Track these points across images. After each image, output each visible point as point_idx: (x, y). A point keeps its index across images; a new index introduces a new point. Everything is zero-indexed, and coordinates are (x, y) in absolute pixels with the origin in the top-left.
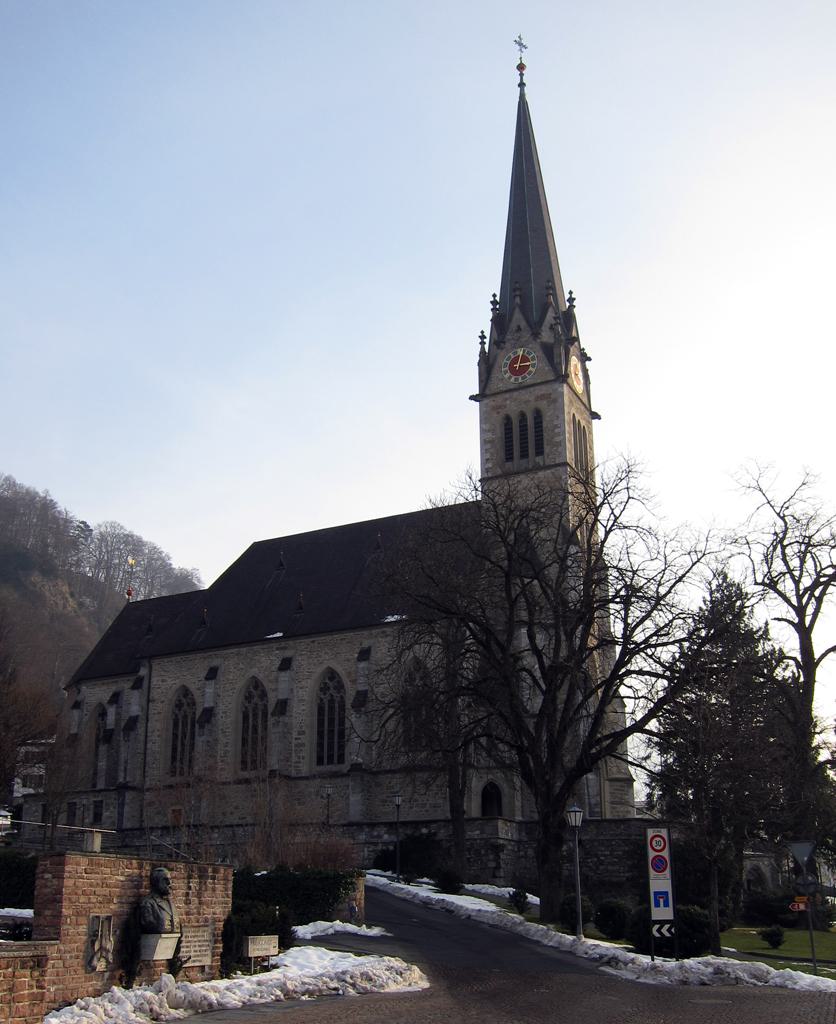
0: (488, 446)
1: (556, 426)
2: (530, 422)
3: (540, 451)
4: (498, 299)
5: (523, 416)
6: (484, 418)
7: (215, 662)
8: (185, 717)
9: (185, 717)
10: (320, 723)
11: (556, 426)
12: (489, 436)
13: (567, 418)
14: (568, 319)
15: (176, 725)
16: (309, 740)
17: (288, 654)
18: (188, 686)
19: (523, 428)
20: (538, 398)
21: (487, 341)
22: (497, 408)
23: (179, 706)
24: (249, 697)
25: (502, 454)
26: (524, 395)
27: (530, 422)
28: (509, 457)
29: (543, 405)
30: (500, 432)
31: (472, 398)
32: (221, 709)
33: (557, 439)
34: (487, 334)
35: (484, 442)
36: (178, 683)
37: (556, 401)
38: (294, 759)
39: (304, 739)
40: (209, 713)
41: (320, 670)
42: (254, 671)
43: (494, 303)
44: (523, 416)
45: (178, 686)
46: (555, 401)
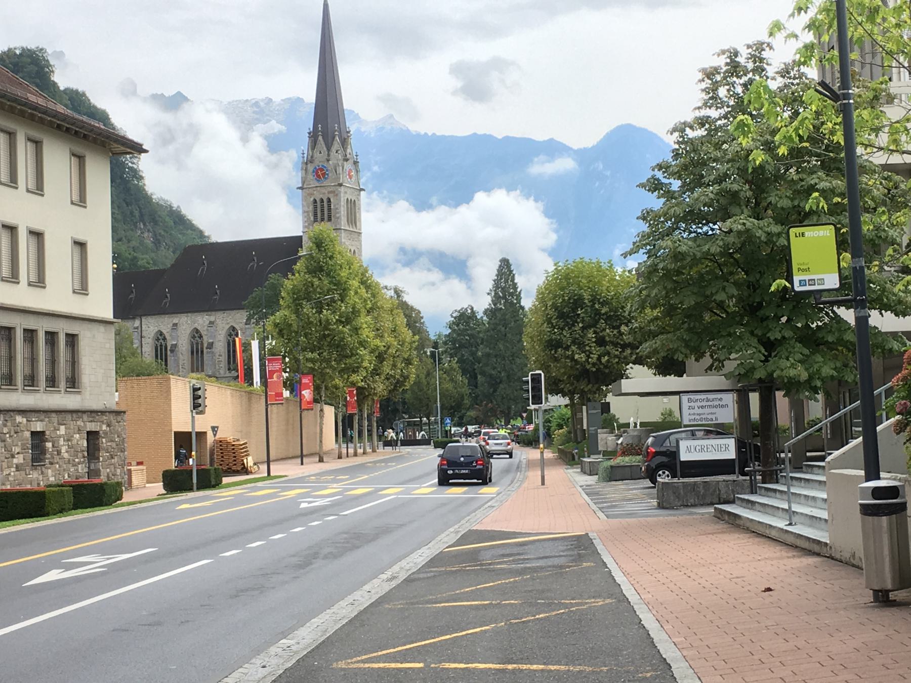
0: (306, 214)
1: (337, 209)
2: (325, 204)
3: (330, 219)
4: (312, 130)
5: (322, 201)
6: (304, 199)
7: (175, 321)
8: (161, 346)
9: (161, 346)
10: (229, 351)
11: (337, 209)
12: (306, 209)
13: (343, 202)
14: (344, 142)
15: (156, 351)
16: (224, 358)
17: (212, 319)
18: (163, 331)
19: (322, 206)
20: (329, 193)
21: (305, 155)
22: (311, 195)
23: (158, 340)
24: (194, 337)
25: (312, 218)
26: (324, 190)
27: (325, 204)
28: (315, 220)
29: (331, 196)
30: (311, 208)
31: (299, 188)
32: (180, 342)
33: (338, 215)
34: (306, 152)
35: (304, 212)
36: (156, 329)
37: (337, 196)
38: (217, 367)
39: (222, 358)
40: (174, 346)
41: (228, 327)
42: (196, 325)
43: (309, 133)
44: (322, 201)
45: (155, 332)
46: (337, 195)
